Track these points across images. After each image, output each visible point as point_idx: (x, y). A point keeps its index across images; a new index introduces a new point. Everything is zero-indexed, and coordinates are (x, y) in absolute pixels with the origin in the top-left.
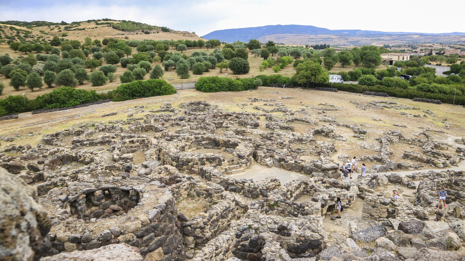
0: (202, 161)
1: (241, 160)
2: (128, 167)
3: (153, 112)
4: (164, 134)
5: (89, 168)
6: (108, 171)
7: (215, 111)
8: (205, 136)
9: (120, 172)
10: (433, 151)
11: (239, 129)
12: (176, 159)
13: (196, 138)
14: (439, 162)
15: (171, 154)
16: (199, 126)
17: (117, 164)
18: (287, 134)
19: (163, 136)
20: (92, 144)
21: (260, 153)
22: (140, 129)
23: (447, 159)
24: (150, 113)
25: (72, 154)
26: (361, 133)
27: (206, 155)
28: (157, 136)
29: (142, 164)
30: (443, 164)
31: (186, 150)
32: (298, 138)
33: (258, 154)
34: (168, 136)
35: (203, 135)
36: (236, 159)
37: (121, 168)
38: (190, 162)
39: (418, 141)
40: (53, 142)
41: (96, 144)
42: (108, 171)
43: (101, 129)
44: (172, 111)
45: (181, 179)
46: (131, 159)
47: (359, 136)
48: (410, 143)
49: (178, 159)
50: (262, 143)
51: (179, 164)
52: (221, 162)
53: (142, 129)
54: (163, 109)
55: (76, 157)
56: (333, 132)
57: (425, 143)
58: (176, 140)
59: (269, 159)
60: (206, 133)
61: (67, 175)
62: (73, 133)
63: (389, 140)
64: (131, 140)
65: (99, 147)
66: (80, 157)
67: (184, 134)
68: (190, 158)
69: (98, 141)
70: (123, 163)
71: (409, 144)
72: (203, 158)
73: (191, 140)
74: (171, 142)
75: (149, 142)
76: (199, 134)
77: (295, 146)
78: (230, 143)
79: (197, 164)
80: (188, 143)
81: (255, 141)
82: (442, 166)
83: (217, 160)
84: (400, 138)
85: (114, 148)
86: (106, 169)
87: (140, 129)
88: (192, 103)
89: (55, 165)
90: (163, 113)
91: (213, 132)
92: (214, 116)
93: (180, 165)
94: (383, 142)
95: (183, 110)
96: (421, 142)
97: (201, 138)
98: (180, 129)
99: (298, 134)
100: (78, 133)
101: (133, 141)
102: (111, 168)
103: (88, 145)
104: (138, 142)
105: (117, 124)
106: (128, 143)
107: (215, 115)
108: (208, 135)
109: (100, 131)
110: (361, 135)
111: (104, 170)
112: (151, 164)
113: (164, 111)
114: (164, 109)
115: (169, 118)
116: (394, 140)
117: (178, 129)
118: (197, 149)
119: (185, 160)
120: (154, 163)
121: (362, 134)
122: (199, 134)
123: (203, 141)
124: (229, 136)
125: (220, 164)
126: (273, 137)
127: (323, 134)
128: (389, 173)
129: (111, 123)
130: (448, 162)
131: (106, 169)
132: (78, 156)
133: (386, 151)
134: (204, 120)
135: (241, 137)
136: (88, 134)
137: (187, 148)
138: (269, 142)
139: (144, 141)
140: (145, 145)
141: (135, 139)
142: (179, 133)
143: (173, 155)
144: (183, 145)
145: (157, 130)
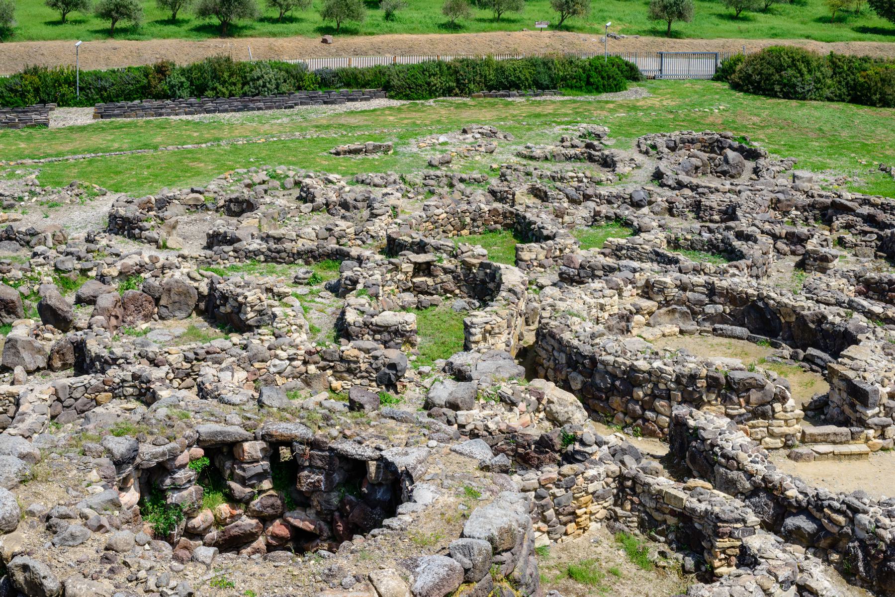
3: (532, 158)
4: (558, 253)
5: (245, 347)
7: (784, 181)
9: (358, 382)
15: (567, 336)
16: (706, 236)
17: (348, 348)
24: (514, 160)
25: (196, 284)
27: (708, 365)
31: (635, 332)
35: (715, 280)
44: (608, 163)
45: (588, 449)
51: (593, 384)
53: (473, 220)
54: (572, 152)
58: (597, 284)
60: (725, 272)
64: (422, 258)
65: (300, 270)
67: (636, 264)
69: (301, 245)
70: (375, 345)
72: (693, 377)
73: (661, 291)
74: (576, 290)
79: (669, 398)
80: (646, 304)
83: (755, 395)
87: (468, 220)
88: (692, 142)
89: (129, 318)
90: (569, 166)
92: (775, 205)
93: (599, 389)
95: (649, 165)
98: (623, 241)
101: (429, 264)
105: (385, 190)
107: (779, 201)
108: (736, 279)
112: (482, 365)
113: (569, 158)
114: (578, 151)
115: (590, 191)
117: (620, 238)
118: (682, 332)
122: (697, 271)
123: (712, 302)
131: (305, 363)
132: (217, 294)
134: (730, 214)
135: (878, 308)
137: (638, 323)
142: (619, 258)
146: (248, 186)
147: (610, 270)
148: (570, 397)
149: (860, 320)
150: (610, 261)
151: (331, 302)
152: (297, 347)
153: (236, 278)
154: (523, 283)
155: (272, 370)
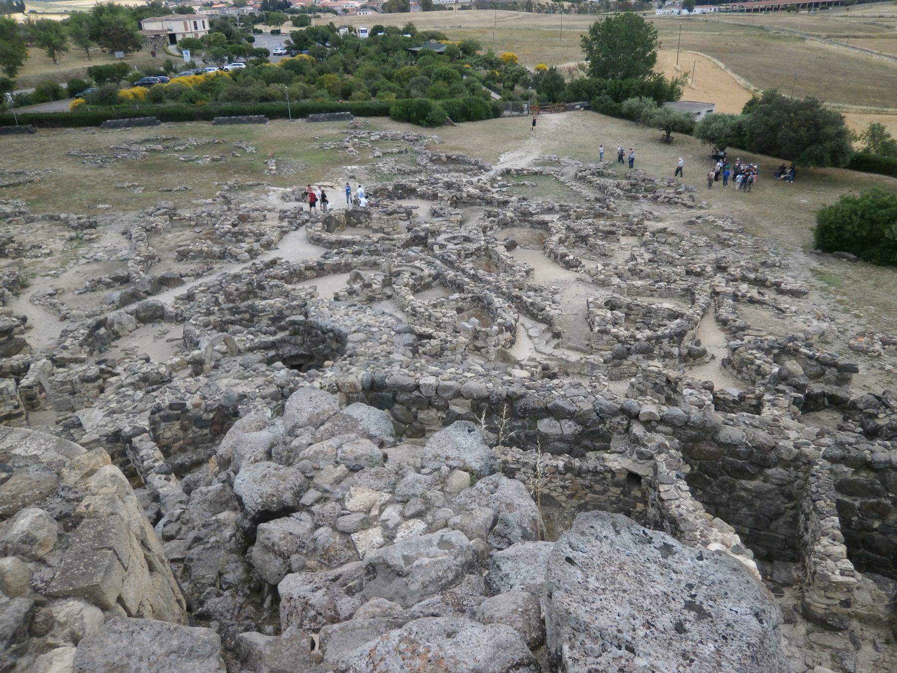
10: (233, 230)
14: (238, 251)
23: (257, 241)
26: (83, 227)
30: (249, 251)
47: (80, 235)
48: (193, 223)
56: (13, 242)
57: (221, 216)
71: (190, 226)
84: (171, 218)
94: (133, 236)
96: (214, 217)
110: (85, 232)
121: (87, 228)
128: (133, 307)
130: (256, 246)
133: (138, 255)
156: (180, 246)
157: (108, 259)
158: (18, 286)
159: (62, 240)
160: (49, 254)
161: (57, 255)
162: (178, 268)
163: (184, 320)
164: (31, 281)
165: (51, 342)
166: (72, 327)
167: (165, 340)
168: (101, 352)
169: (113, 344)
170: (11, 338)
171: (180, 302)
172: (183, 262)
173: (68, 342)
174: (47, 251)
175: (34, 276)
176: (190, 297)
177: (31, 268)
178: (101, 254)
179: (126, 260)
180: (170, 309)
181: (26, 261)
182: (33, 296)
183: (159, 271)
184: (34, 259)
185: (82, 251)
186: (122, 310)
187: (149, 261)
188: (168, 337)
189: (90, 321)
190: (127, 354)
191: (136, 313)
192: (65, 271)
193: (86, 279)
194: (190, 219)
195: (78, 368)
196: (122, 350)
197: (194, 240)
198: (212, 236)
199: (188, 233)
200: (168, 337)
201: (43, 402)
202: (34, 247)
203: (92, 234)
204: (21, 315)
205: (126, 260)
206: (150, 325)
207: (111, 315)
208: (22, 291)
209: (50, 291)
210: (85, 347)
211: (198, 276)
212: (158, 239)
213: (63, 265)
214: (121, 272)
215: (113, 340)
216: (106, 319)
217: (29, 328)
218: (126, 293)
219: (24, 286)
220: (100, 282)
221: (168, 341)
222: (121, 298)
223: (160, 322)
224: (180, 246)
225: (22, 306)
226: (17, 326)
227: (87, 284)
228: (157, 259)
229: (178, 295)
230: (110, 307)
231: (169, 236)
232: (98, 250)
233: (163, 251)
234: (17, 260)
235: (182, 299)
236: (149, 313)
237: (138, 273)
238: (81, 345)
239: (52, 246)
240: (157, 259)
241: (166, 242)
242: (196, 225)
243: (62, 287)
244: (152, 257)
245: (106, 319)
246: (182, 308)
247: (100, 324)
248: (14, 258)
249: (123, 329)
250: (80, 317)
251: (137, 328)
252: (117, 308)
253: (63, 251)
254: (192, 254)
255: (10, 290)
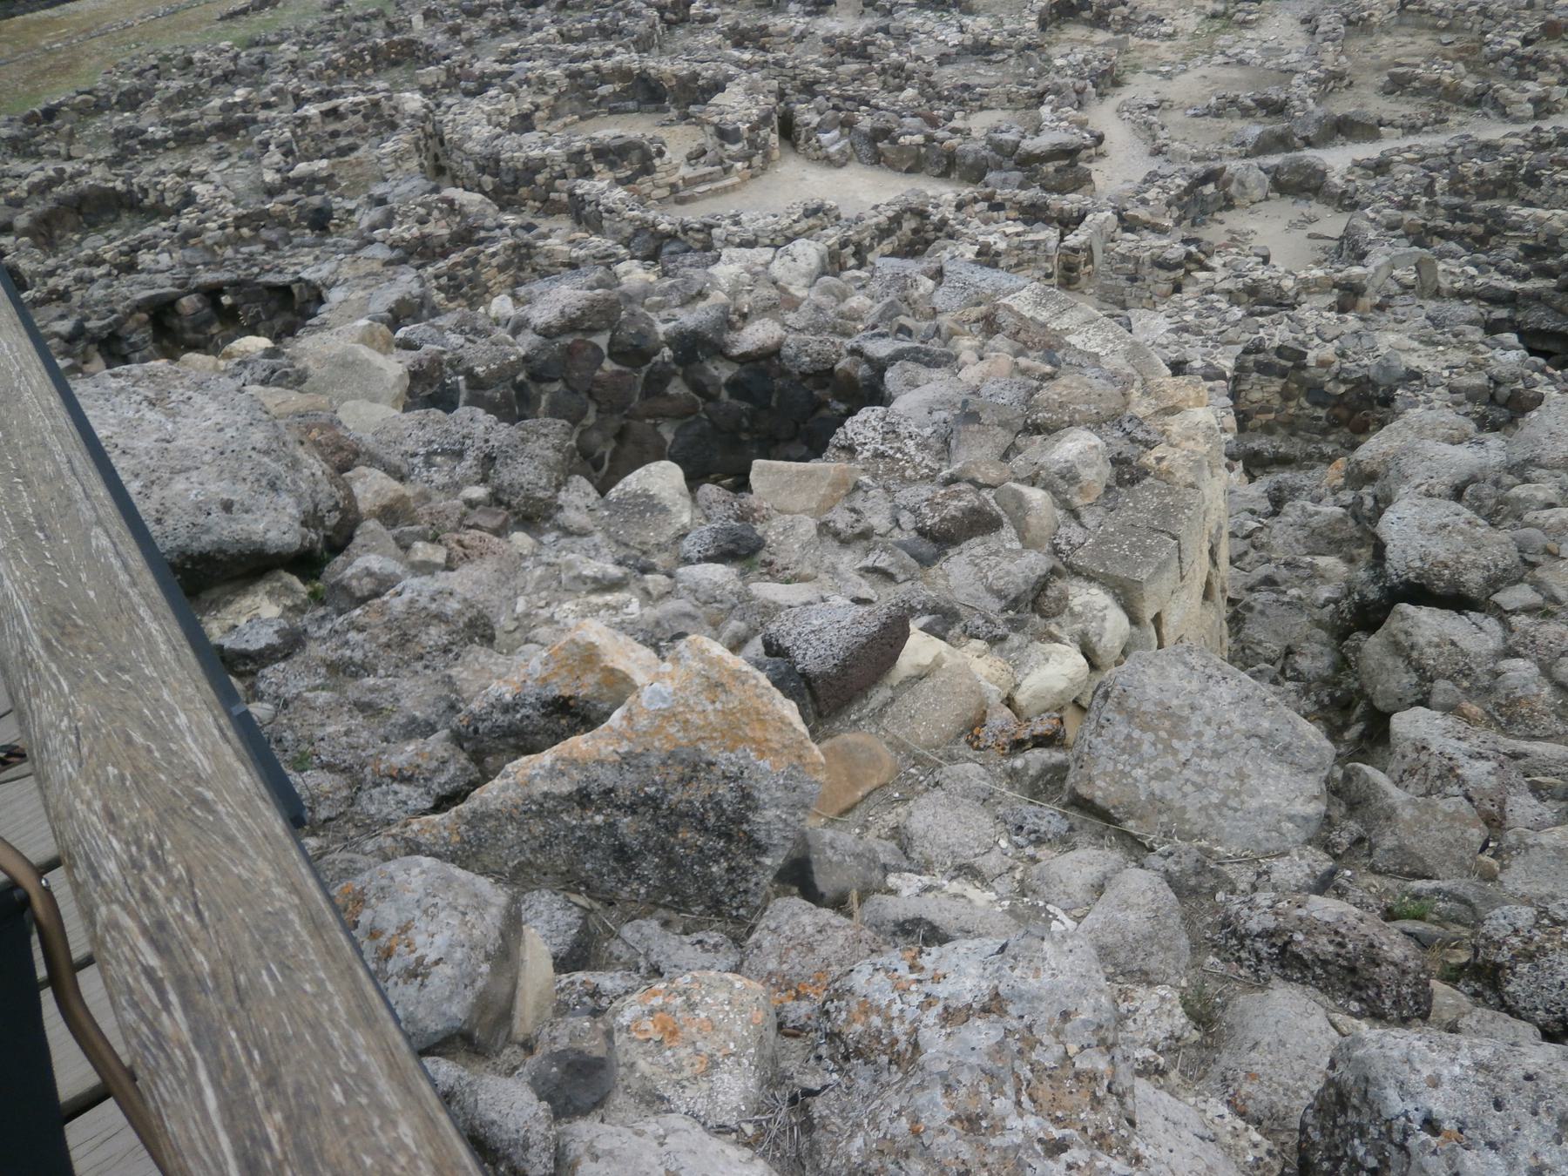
0: (581, 164)
1: (727, 146)
2: (319, 211)
5: (175, 229)
6: (245, 231)
8: (606, 65)
10: (1520, 51)
11: (744, 25)
12: (490, 164)
13: (572, 75)
14: (1514, 95)
15: (469, 145)
18: (938, 28)
19: (453, 81)
20: (187, 138)
21: (807, 114)
22: (368, 58)
28: (428, 81)
29: (370, 197)
32: (976, 41)
33: (798, 120)
34: (469, 77)
36: (711, 142)
37: (293, 218)
38: (538, 172)
39: (1478, 13)
40: (38, 145)
41: (200, 138)
42: (245, 231)
43: (218, 72)
46: (329, 181)
48: (1442, 23)
49: (497, 161)
50: (824, 71)
52: (651, 159)
53: (373, 57)
55: (130, 192)
57: (1507, 16)
58: (492, 92)
59: (835, 133)
61: (104, 262)
62: (114, 100)
63: (1353, 17)
64: (326, 106)
65: (214, 144)
66: (145, 192)
67: (529, 64)
68: (536, 153)
69: (205, 123)
71: (1435, 28)
73: (554, 84)
74: (475, 102)
75: (395, 108)
76: (585, 57)
77: (948, 76)
78: (700, 82)
80: (541, 100)
81: (794, 67)
82: (1529, 108)
85: (265, 145)
86: (237, 228)
87: (368, 58)
91: (643, 45)
94: (1321, 29)
97: (592, 73)
98: (515, 45)
99: (979, 25)
100: (131, 101)
102: (256, 220)
103: (172, 144)
104: (355, 112)
106: (318, 120)
109: (215, 82)
111: (230, 230)
116: (1374, 19)
119: (520, 166)
120: (407, 186)
122: (585, 57)
123: (603, 82)
124: (700, 55)
125: (647, 169)
126: (873, 43)
127: (1086, 14)
128: (1274, 160)
129: (257, 44)
132: (135, 188)
133: (1316, 67)
135: (747, 56)
136: (169, 103)
138: (853, 66)
139: (376, 104)
140: (382, 120)
141: (344, 103)
143: (478, 149)
144: (527, 106)
145: (429, 56)
146: (139, 74)
147: (504, 76)
148: (478, 197)
149: (732, 70)
150: (505, 67)
151: (245, 168)
152: (224, 216)
153: (149, 168)
154: (426, 106)
155: (209, 242)
156: (1400, 65)
157: (1262, 64)
158: (1108, 80)
159: (1198, 14)
160: (1170, 36)
161: (1182, 40)
162: (1380, 107)
163: (1354, 206)
164: (1129, 77)
165: (1127, 186)
166: (1167, 169)
167: (1306, 232)
168: (1193, 224)
169: (1218, 216)
170: (1073, 165)
171: (1359, 171)
172: (1392, 98)
173: (1151, 194)
174: (1170, 30)
175: (1136, 68)
176: (1381, 167)
177: (1136, 54)
178: (1253, 52)
179: (1293, 72)
180: (1337, 180)
181: (1134, 41)
182: (1124, 103)
183: (1342, 106)
184: (1145, 41)
185: (1222, 40)
186: (1254, 162)
187: (1333, 81)
188: (1312, 229)
189: (1198, 168)
190: (1233, 239)
191: (1274, 173)
192: (1185, 71)
193: (1213, 93)
194: (1440, 14)
195: (1152, 241)
196: (1229, 231)
197: (1431, 58)
198: (1472, 57)
199: (1425, 42)
200: (1312, 229)
201: (1084, 279)
202: (1152, 18)
203: (1250, 13)
204: (1098, 131)
205: (1293, 72)
206: (1289, 200)
207: (1233, 166)
208: (1111, 90)
209: (1152, 100)
210: (1174, 208)
211: (1413, 129)
212: (1363, 42)
213: (1189, 57)
214: (1275, 93)
215: (1220, 210)
216: (1223, 169)
217: (1102, 155)
218: (1271, 132)
219: (1117, 84)
220: (1233, 102)
221: (1310, 236)
222: (1260, 137)
223: (1308, 199)
224: (1400, 65)
225: (1104, 116)
226: (1087, 147)
227: (1213, 101)
228: (1346, 82)
229: (1359, 157)
230: (1235, 150)
231: (1386, 41)
232: (1249, 44)
233: (1363, 68)
234: (1121, 36)
235: (1364, 167)
236: (1297, 179)
237: (1303, 101)
238: (1169, 204)
239: (1180, 23)
240: (1346, 82)
241: (1375, 52)
242: (1447, 29)
243: (1172, 97)
244: (1337, 76)
245: (1223, 169)
246: (1358, 183)
247: (1210, 176)
248: (1116, 33)
249: (1243, 194)
250: (1183, 155)
251: (1267, 199)
252: (1246, 156)
253: (1194, 35)
254: (1417, 84)
255: (1095, 85)
